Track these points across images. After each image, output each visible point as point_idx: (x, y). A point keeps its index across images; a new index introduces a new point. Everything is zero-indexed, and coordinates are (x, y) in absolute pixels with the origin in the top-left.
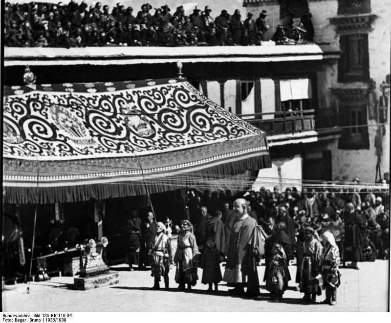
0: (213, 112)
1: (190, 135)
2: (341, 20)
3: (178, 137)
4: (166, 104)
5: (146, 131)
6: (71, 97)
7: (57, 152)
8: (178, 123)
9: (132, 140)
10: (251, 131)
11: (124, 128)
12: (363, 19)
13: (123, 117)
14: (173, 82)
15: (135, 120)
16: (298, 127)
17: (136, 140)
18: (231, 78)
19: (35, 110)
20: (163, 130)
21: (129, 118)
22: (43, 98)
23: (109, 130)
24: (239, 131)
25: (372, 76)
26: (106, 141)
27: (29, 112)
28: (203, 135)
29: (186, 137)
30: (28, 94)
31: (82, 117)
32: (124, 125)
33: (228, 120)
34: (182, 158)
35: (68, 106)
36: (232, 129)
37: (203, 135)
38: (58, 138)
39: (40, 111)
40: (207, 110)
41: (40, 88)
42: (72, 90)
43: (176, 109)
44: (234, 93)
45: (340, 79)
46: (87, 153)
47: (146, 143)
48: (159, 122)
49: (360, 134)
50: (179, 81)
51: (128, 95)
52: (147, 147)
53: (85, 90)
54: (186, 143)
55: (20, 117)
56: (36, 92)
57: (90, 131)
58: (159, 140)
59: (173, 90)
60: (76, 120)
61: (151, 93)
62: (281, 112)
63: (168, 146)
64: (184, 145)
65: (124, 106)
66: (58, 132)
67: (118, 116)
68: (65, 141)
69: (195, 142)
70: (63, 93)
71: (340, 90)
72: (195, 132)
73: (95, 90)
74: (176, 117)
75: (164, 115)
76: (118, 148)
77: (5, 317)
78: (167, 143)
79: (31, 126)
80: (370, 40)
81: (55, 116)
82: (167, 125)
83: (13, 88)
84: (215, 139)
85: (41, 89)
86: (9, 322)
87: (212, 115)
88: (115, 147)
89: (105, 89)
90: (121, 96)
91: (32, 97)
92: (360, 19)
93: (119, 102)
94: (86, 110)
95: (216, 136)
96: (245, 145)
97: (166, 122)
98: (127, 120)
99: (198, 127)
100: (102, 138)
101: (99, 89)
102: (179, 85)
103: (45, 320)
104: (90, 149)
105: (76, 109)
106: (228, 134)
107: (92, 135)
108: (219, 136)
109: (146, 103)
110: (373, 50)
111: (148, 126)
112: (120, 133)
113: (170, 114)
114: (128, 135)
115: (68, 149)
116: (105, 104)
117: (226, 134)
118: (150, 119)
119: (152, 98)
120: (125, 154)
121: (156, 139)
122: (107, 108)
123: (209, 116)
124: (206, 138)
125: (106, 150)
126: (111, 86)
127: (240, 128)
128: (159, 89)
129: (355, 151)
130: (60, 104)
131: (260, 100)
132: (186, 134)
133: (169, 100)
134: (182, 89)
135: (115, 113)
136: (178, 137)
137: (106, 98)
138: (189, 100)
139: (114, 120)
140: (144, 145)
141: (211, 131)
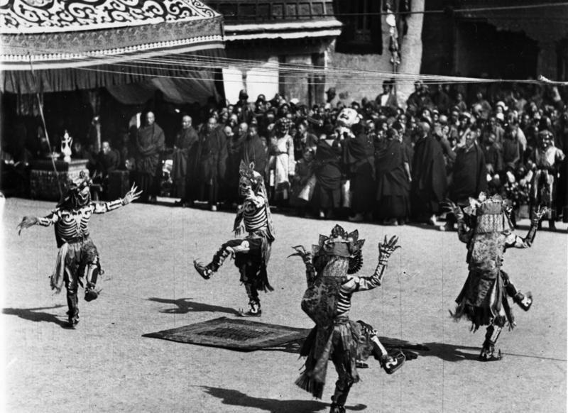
1: (106, 9)
3: (88, 11)
10: (200, 11)
17: (23, 11)
24: (182, 10)
28: (127, 10)
34: (92, 43)
36: (172, 6)
37: (127, 10)
47: (38, 16)
49: (369, 31)
52: (40, 22)
54: (99, 20)
58: (58, 13)
63: (71, 22)
64: (96, 23)
69: (113, 20)
72: (114, 5)
78: (71, 18)
84: (146, 18)
95: (146, 14)
96: (189, 31)
106: (166, 13)
108: (150, 14)
117: (161, 12)
121: (53, 10)
124: (131, 15)
132: (101, 7)
136: (88, 11)
140: (36, 19)
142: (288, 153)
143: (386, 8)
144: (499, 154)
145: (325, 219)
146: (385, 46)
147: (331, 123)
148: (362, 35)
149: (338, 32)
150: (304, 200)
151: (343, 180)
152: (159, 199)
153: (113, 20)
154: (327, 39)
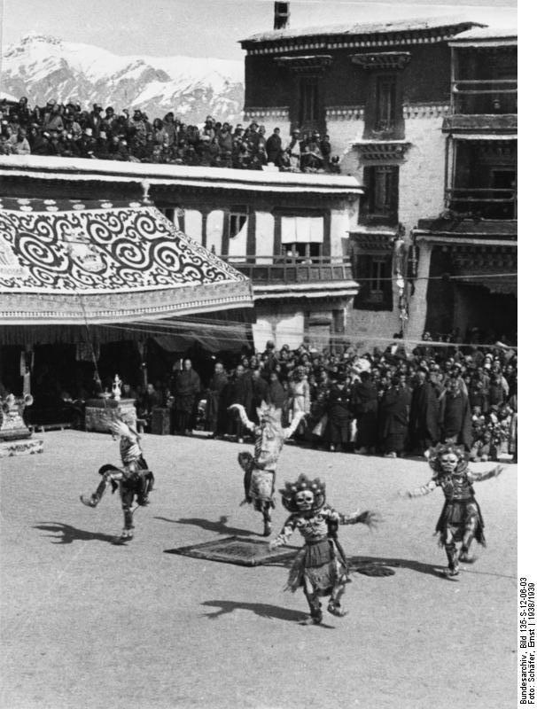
0: (186, 248)
1: (152, 273)
2: (366, 146)
3: (136, 276)
5: (96, 264)
8: (139, 258)
9: (75, 275)
10: (232, 275)
11: (66, 258)
12: (394, 147)
14: (135, 206)
15: (81, 250)
16: (300, 277)
17: (80, 275)
18: (215, 207)
20: (117, 265)
21: (74, 246)
23: (45, 260)
24: (216, 275)
26: (40, 273)
28: (170, 275)
29: (146, 275)
31: (10, 240)
33: (204, 259)
36: (209, 271)
37: (170, 275)
40: (177, 245)
43: (136, 240)
46: (12, 286)
47: (93, 280)
48: (113, 255)
49: (380, 292)
50: (144, 205)
52: (94, 285)
53: (17, 207)
54: (146, 283)
57: (20, 259)
58: (110, 278)
59: (134, 215)
61: (105, 218)
62: (280, 257)
63: (121, 285)
64: (142, 285)
65: (67, 231)
67: (59, 243)
69: (157, 283)
73: (30, 208)
75: (120, 246)
76: (56, 283)
78: (121, 282)
80: (401, 174)
82: (123, 259)
84: (185, 281)
87: (183, 251)
88: (52, 281)
89: (44, 208)
90: (65, 218)
92: (390, 148)
93: (62, 225)
94: (17, 232)
95: (186, 278)
96: (223, 292)
97: (122, 255)
99: (164, 265)
100: (35, 269)
102: (143, 210)
104: (17, 281)
106: (203, 277)
107: (22, 264)
109: (98, 230)
110: (404, 186)
113: (129, 245)
114: (70, 267)
116: (43, 227)
117: (199, 276)
118: (101, 250)
119: (106, 224)
120: (64, 291)
121: (106, 275)
122: (45, 231)
123: (180, 252)
124: (173, 279)
126: (53, 205)
127: (218, 270)
128: (116, 214)
129: (373, 313)
131: (254, 239)
132: (148, 272)
133: (129, 228)
134: (147, 215)
135: (55, 240)
136: (136, 276)
137: (45, 219)
140: (91, 282)
141: (180, 271)
142: (304, 395)
143: (396, 273)
144: (486, 399)
145: (335, 451)
146: (395, 304)
147: (341, 373)
148: (376, 295)
149: (355, 292)
150: (317, 436)
151: (351, 419)
152: (195, 432)
153: (157, 283)
154: (346, 298)
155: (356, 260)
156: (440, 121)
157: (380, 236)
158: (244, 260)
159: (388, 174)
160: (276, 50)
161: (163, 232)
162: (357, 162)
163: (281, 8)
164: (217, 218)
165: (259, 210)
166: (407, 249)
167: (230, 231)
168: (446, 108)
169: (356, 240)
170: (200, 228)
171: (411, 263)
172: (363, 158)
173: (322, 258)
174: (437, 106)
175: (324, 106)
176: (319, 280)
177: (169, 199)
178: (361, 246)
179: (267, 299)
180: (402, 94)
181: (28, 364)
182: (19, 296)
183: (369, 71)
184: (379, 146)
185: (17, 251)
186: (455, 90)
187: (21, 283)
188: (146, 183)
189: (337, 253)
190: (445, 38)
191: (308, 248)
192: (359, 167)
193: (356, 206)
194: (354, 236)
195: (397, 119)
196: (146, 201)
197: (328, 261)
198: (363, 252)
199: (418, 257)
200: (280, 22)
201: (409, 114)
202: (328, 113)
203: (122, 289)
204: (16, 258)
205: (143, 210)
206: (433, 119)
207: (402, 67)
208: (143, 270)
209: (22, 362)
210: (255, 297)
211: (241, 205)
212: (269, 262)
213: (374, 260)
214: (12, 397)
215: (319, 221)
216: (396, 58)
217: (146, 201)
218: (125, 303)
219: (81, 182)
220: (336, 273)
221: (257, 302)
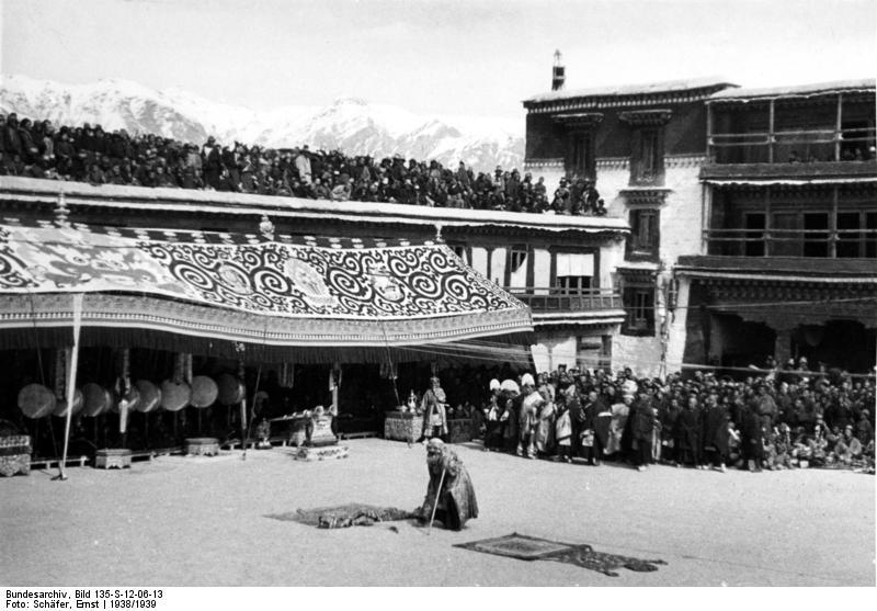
0: (473, 280)
2: (631, 192)
4: (420, 267)
5: (395, 294)
6: (312, 251)
7: (290, 308)
8: (432, 289)
9: (378, 303)
11: (369, 289)
12: (656, 192)
13: (369, 277)
14: (429, 244)
15: (382, 282)
16: (572, 307)
17: (381, 304)
18: (501, 246)
19: (270, 262)
20: (413, 294)
22: (281, 250)
23: (352, 290)
25: (661, 257)
26: (347, 301)
27: (263, 262)
28: (459, 303)
30: (263, 244)
31: (322, 273)
32: (371, 286)
35: (308, 261)
36: (493, 300)
37: (459, 303)
38: (293, 293)
39: (276, 263)
41: (277, 239)
42: (314, 244)
43: (430, 273)
44: (504, 263)
45: (628, 257)
46: (323, 313)
48: (410, 286)
50: (436, 243)
51: (377, 254)
52: (394, 312)
53: (329, 245)
54: (438, 311)
55: (252, 267)
56: (274, 243)
58: (407, 306)
59: (429, 252)
60: (316, 276)
61: (403, 254)
65: (371, 265)
66: (293, 287)
67: (364, 276)
68: (300, 297)
69: (448, 310)
70: (303, 247)
71: (626, 269)
73: (339, 246)
74: (430, 282)
75: (416, 279)
76: (361, 310)
77: (11, 598)
78: (417, 309)
79: (263, 277)
81: (292, 270)
82: (418, 290)
83: (248, 236)
84: (472, 309)
85: (279, 240)
86: (20, 609)
87: (470, 283)
88: (357, 308)
89: (351, 246)
90: (370, 254)
91: (268, 247)
93: (367, 260)
96: (505, 318)
97: (418, 286)
98: (373, 282)
100: (343, 298)
101: (345, 245)
102: (436, 247)
103: (109, 604)
105: (317, 264)
106: (488, 305)
107: (332, 294)
108: (477, 306)
109: (397, 265)
111: (397, 289)
112: (364, 294)
113: (424, 278)
114: (373, 297)
115: (303, 306)
116: (351, 262)
117: (485, 305)
118: (399, 282)
119: (404, 259)
120: (367, 317)
121: (404, 303)
122: (352, 266)
125: (346, 310)
130: (299, 258)
132: (439, 301)
133: (423, 263)
134: (440, 252)
137: (352, 255)
138: (446, 264)
139: (359, 279)
140: (390, 309)
141: (468, 300)
143: (658, 303)
146: (657, 330)
148: (641, 323)
149: (622, 320)
153: (448, 310)
154: (613, 325)
155: (622, 291)
156: (697, 171)
157: (644, 270)
158: (524, 291)
159: (651, 217)
160: (554, 109)
161: (454, 266)
162: (623, 207)
163: (559, 71)
164: (500, 254)
165: (538, 247)
166: (668, 282)
167: (511, 266)
168: (703, 159)
169: (623, 274)
170: (486, 263)
171: (671, 295)
172: (629, 203)
173: (592, 289)
174: (694, 157)
175: (595, 157)
176: (590, 309)
177: (460, 238)
178: (627, 280)
179: (545, 326)
180: (663, 147)
181: (336, 380)
182: (328, 322)
183: (635, 127)
184: (643, 192)
185: (328, 282)
186: (711, 142)
187: (330, 310)
188: (439, 225)
189: (607, 284)
190: (703, 97)
191: (580, 282)
192: (625, 211)
193: (623, 243)
194: (621, 271)
195: (657, 169)
196: (438, 239)
197: (598, 293)
198: (629, 285)
199: (677, 289)
200: (557, 84)
201: (669, 164)
202: (598, 164)
203: (417, 316)
204: (327, 289)
205: (436, 247)
206: (691, 168)
207: (662, 123)
208: (435, 299)
209: (331, 379)
210: (535, 324)
211: (521, 242)
212: (546, 293)
213: (639, 292)
214: (321, 408)
215: (590, 258)
216: (658, 115)
217: (438, 239)
218: (420, 328)
219: (384, 224)
220: (605, 303)
221: (535, 327)
